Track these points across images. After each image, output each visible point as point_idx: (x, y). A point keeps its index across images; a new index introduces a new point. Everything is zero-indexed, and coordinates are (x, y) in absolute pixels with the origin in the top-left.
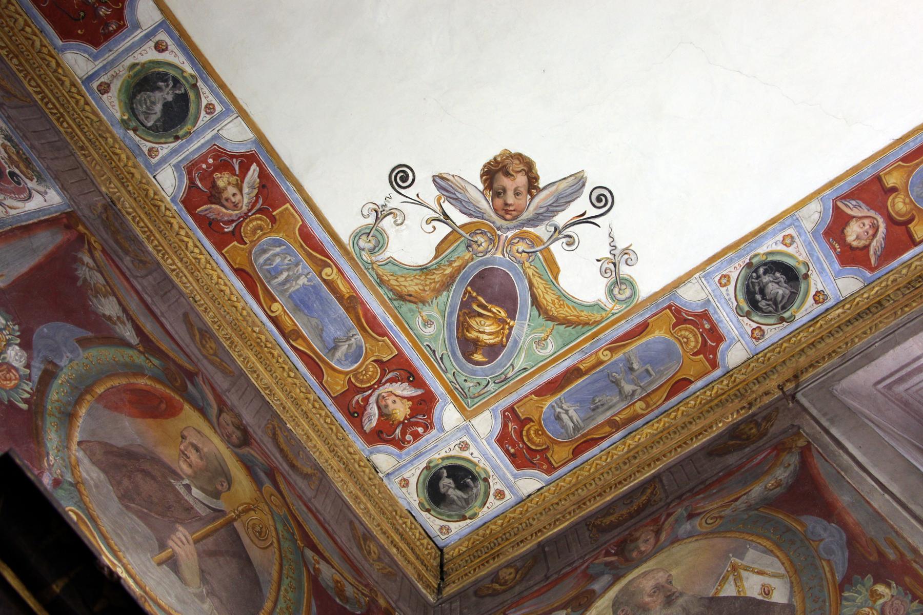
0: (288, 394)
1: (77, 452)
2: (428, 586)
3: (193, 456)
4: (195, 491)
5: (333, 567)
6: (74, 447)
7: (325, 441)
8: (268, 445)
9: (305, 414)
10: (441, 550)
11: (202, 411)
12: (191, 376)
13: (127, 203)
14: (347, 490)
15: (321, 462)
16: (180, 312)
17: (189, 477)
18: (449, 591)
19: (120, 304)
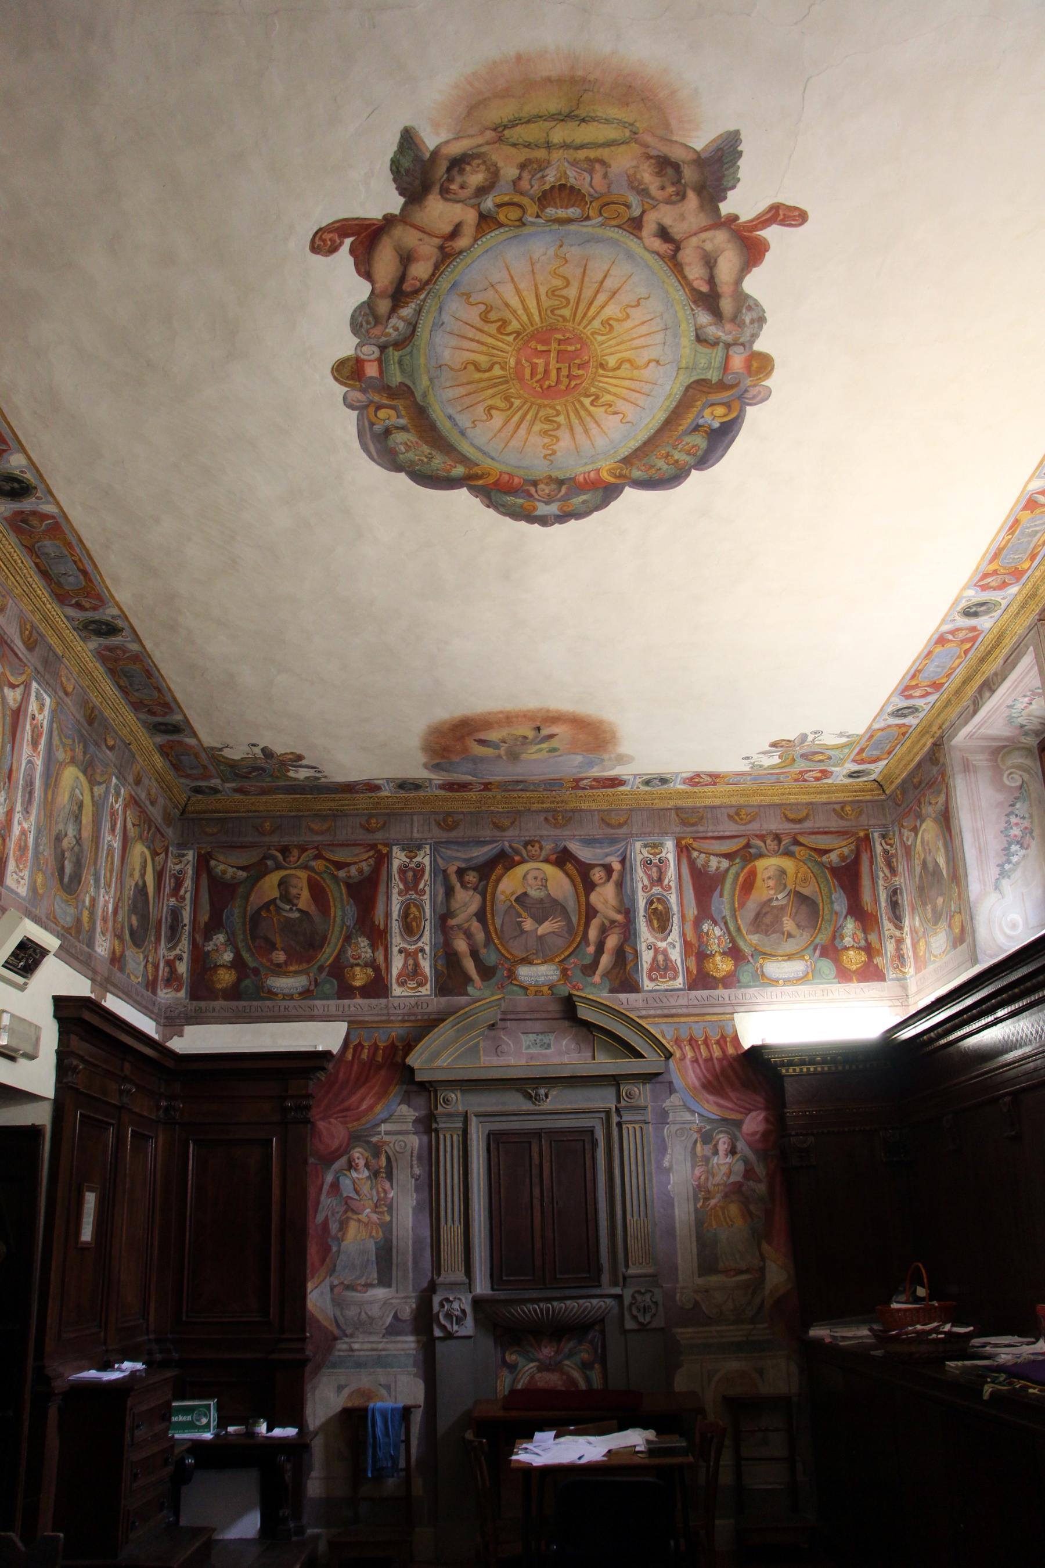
0: (778, 795)
1: (748, 937)
2: (879, 795)
3: (771, 883)
4: (780, 897)
5: (835, 849)
6: (746, 937)
7: (804, 794)
8: (786, 827)
9: (789, 794)
10: (875, 780)
11: (761, 856)
12: (748, 845)
13: (680, 803)
14: (824, 798)
15: (808, 801)
16: (727, 819)
17: (775, 894)
18: (887, 792)
19: (713, 855)
